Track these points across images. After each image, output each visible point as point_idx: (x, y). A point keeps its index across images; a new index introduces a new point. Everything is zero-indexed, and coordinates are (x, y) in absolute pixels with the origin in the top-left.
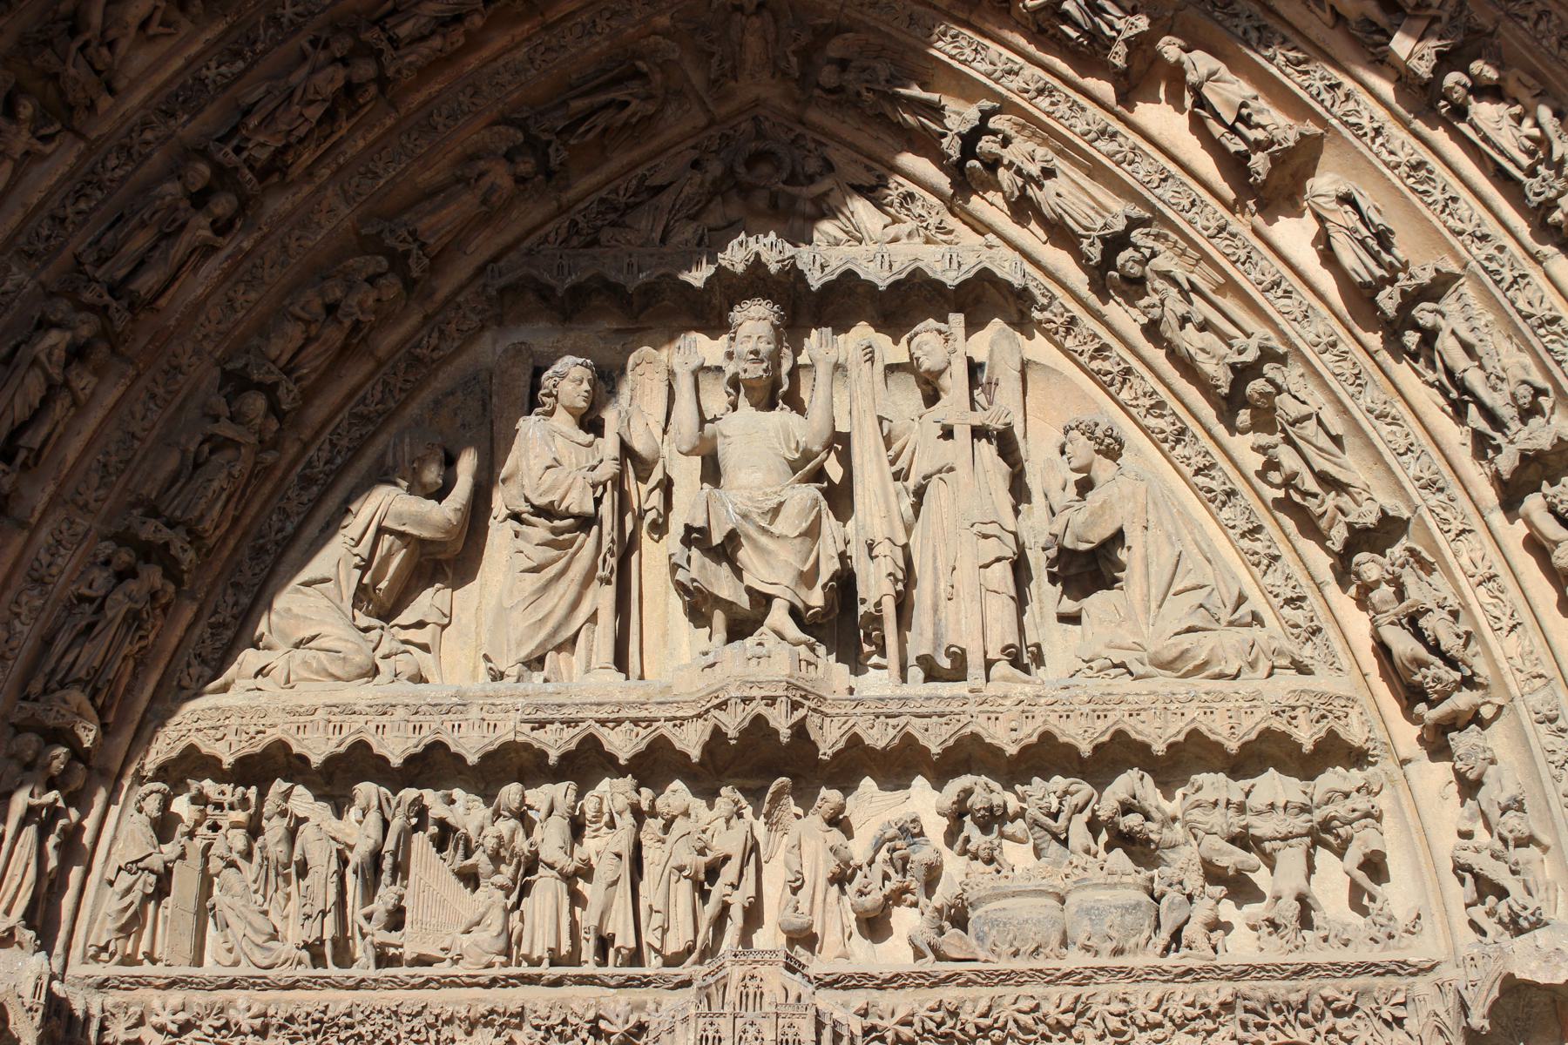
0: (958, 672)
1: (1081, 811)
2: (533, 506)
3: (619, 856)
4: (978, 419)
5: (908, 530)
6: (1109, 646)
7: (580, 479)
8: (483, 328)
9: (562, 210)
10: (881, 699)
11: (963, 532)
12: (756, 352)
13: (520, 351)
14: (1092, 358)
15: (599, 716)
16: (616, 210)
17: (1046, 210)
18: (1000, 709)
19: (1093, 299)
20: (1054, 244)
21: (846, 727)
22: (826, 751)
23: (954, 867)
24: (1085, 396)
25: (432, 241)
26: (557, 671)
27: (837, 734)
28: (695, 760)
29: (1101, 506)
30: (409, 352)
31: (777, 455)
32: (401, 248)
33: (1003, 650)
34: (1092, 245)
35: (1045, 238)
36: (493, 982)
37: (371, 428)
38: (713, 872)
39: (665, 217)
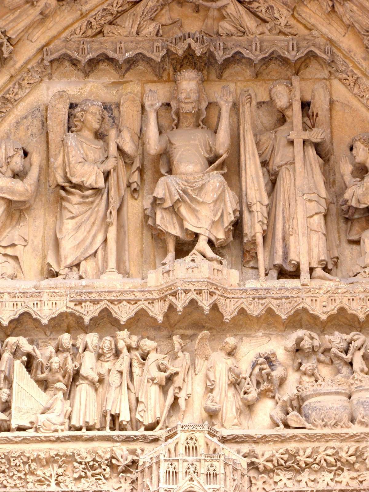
0: (295, 274)
1: (359, 349)
3: (121, 373)
4: (306, 135)
9: (83, 16)
10: (256, 290)
13: (62, 95)
15: (108, 298)
16: (112, 14)
17: (345, 19)
18: (318, 295)
21: (237, 305)
22: (228, 317)
23: (293, 377)
25: (13, 37)
27: (233, 308)
28: (160, 322)
36: (58, 440)
38: (170, 379)
39: (139, 19)
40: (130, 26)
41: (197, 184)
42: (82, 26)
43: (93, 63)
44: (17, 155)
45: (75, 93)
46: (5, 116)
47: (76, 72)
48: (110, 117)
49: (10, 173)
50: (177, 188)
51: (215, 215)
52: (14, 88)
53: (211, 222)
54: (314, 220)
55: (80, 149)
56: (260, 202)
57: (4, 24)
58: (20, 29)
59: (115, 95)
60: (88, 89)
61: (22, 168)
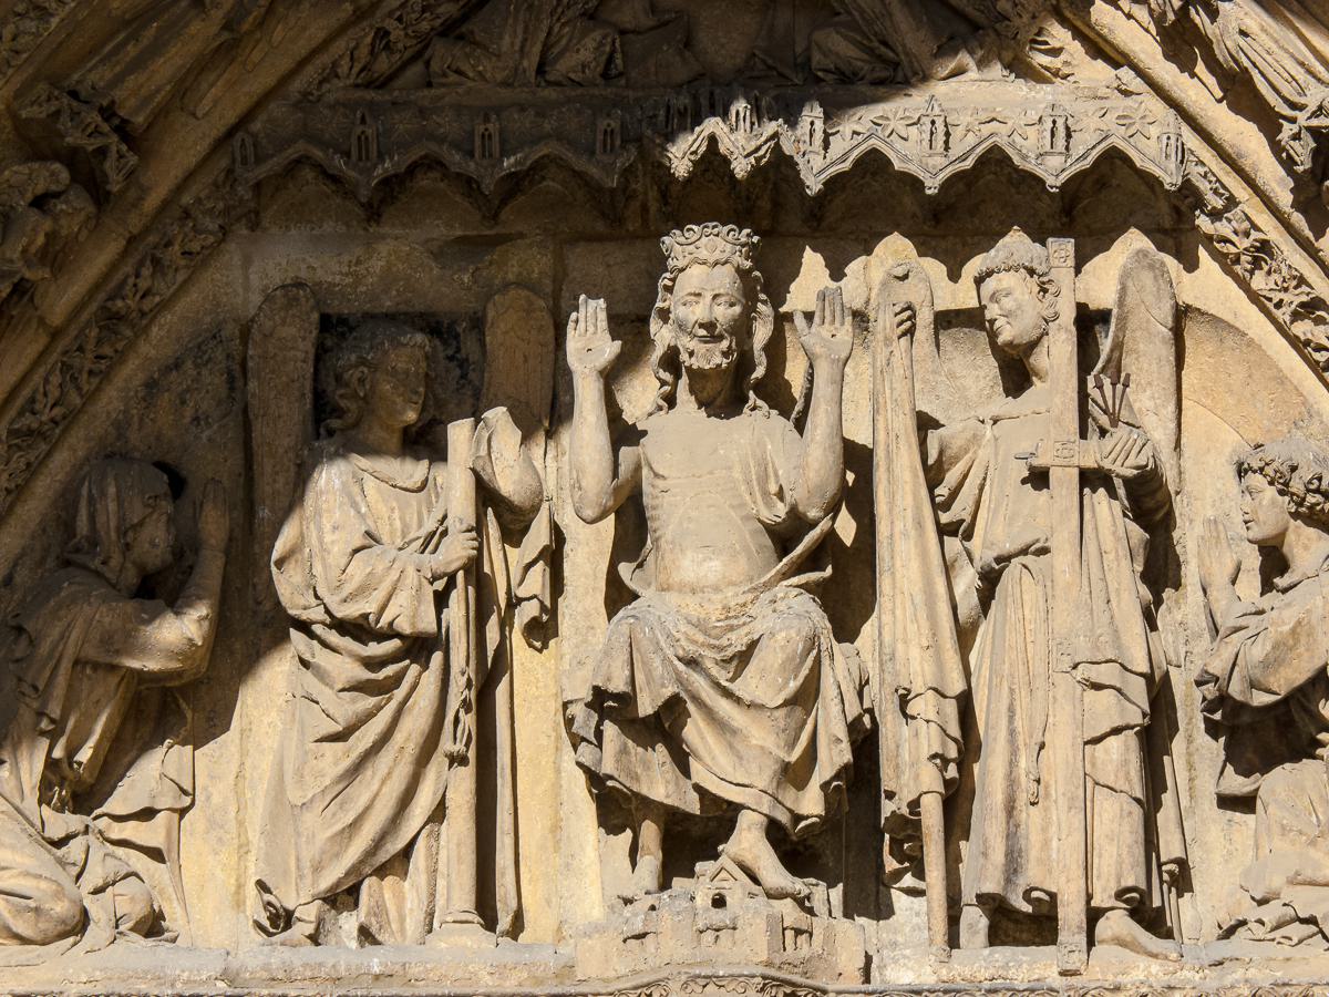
2: (327, 611)
4: (1093, 453)
5: (965, 636)
6: (1292, 882)
7: (411, 571)
8: (224, 232)
11: (1058, 678)
12: (710, 326)
14: (1296, 316)
19: (1298, 220)
20: (1232, 107)
24: (1281, 379)
26: (379, 910)
29: (1293, 631)
30: (103, 308)
31: (747, 518)
32: (92, 145)
33: (1119, 895)
34: (1296, 137)
35: (1220, 94)
37: (44, 447)
40: (517, 48)
41: (733, 636)
42: (355, 48)
43: (392, 188)
44: (155, 516)
45: (338, 279)
46: (110, 368)
47: (338, 201)
48: (451, 358)
49: (131, 577)
50: (670, 653)
51: (792, 745)
52: (137, 275)
53: (777, 767)
54: (1107, 751)
55: (359, 499)
56: (936, 690)
57: (108, 75)
58: (158, 91)
59: (469, 289)
60: (377, 265)
61: (169, 558)
